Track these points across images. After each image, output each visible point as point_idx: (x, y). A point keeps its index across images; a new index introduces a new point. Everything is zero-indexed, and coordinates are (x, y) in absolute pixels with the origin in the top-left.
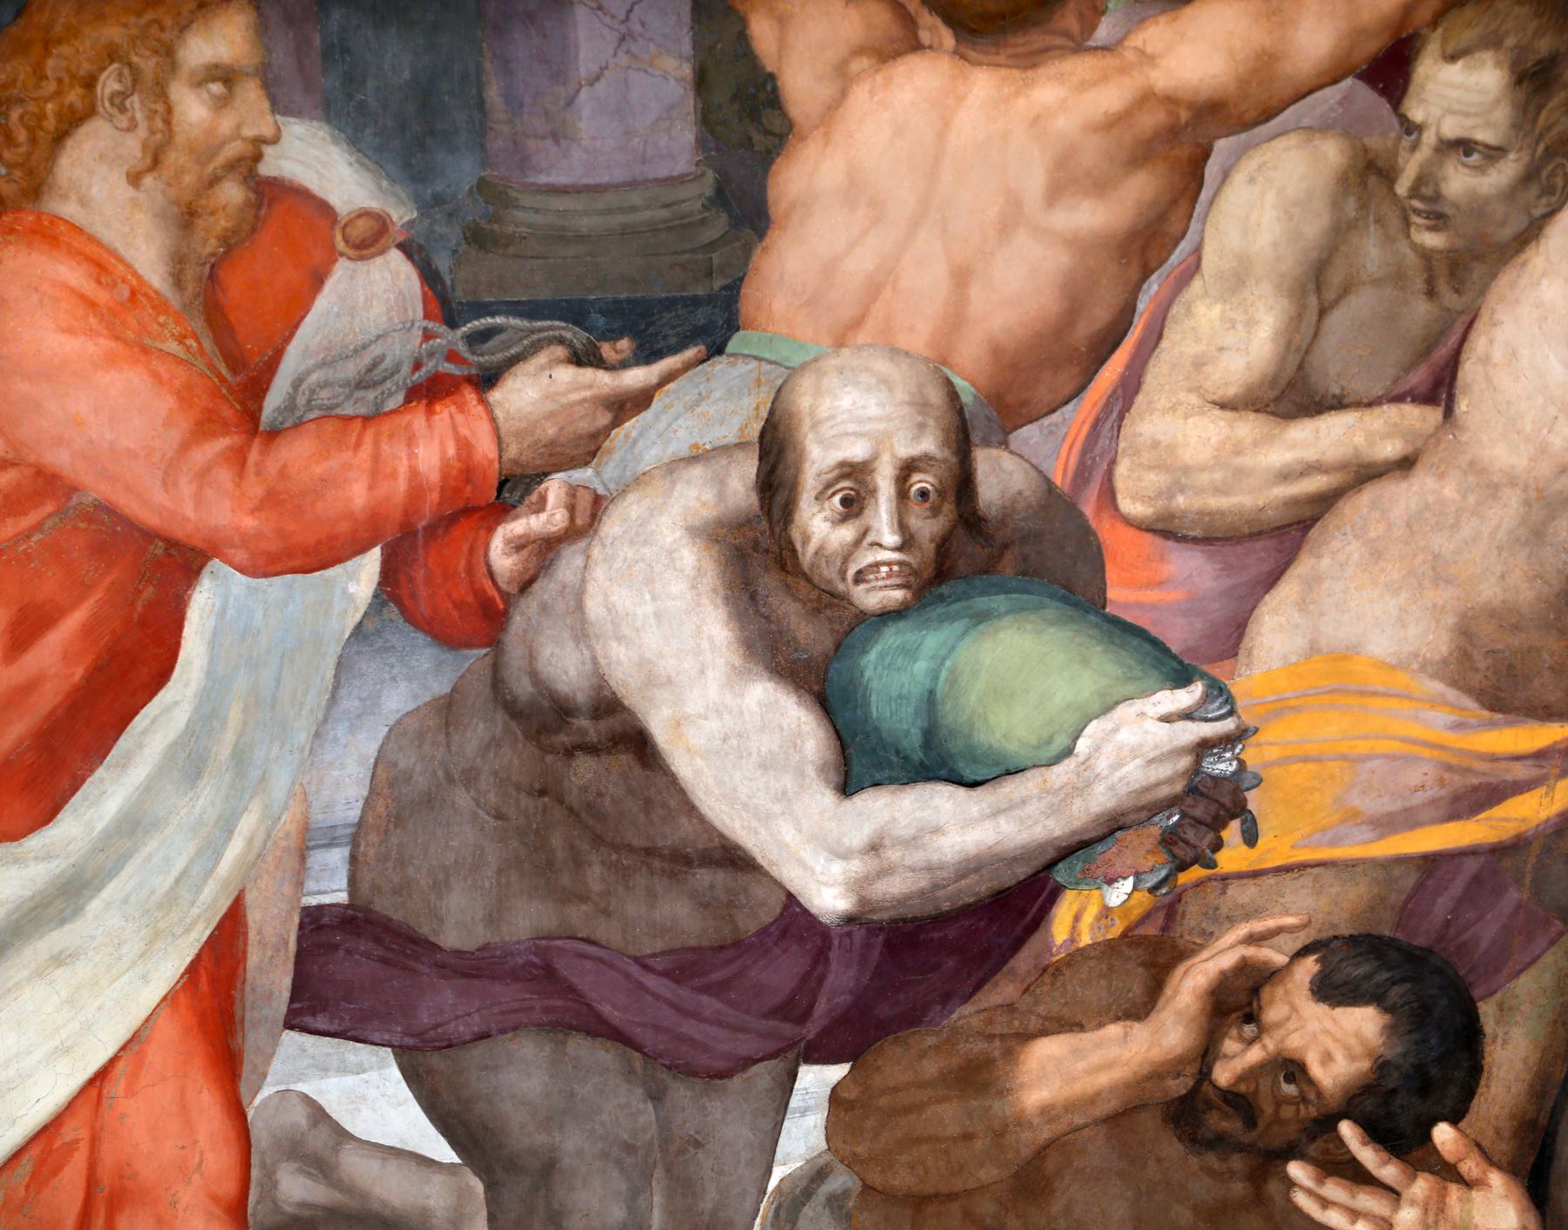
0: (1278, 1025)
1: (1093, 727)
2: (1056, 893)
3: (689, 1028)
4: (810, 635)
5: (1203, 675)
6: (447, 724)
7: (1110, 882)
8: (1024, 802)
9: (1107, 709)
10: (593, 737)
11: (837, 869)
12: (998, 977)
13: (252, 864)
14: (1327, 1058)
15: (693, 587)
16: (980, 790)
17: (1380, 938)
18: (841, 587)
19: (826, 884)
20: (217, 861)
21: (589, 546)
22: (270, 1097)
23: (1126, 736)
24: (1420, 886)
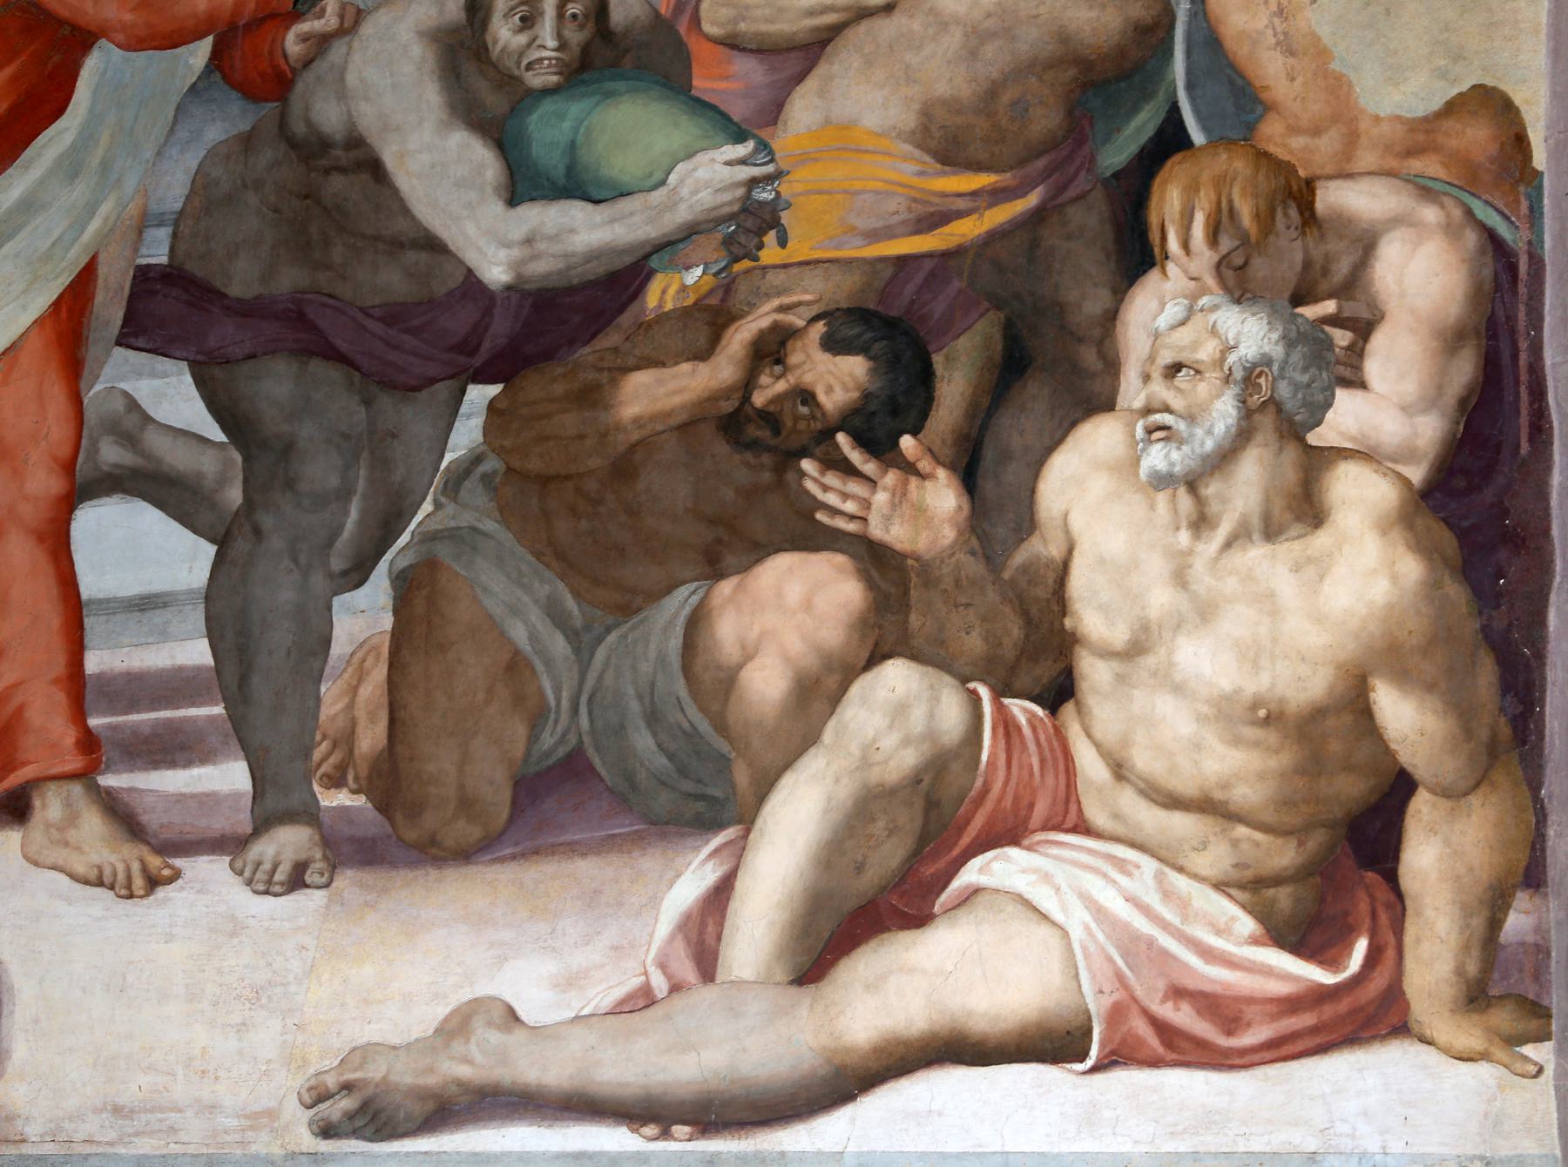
0: (798, 366)
1: (679, 167)
2: (651, 274)
3: (393, 356)
4: (494, 102)
5: (754, 136)
6: (246, 150)
7: (687, 268)
8: (632, 214)
9: (690, 156)
10: (344, 162)
11: (503, 254)
12: (608, 329)
13: (106, 235)
14: (829, 390)
15: (419, 69)
16: (602, 205)
17: (867, 310)
18: (516, 73)
19: (494, 264)
20: (82, 232)
21: (351, 40)
22: (100, 392)
23: (702, 174)
24: (894, 277)
